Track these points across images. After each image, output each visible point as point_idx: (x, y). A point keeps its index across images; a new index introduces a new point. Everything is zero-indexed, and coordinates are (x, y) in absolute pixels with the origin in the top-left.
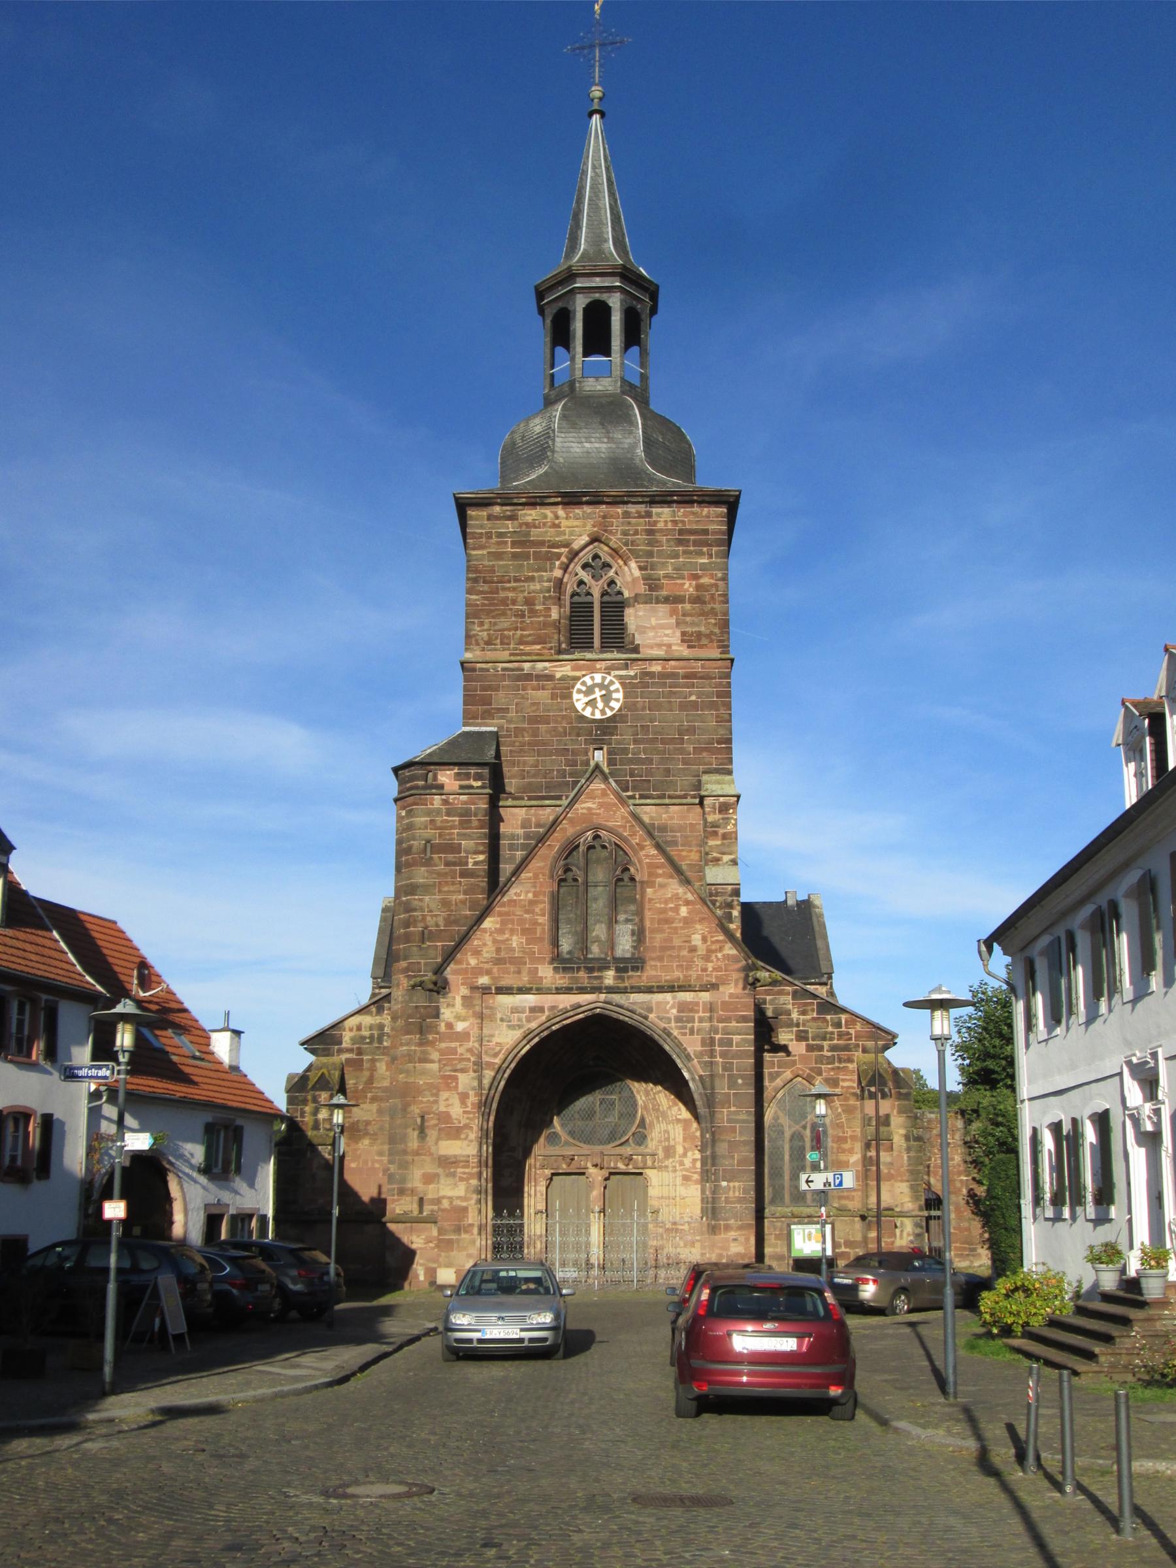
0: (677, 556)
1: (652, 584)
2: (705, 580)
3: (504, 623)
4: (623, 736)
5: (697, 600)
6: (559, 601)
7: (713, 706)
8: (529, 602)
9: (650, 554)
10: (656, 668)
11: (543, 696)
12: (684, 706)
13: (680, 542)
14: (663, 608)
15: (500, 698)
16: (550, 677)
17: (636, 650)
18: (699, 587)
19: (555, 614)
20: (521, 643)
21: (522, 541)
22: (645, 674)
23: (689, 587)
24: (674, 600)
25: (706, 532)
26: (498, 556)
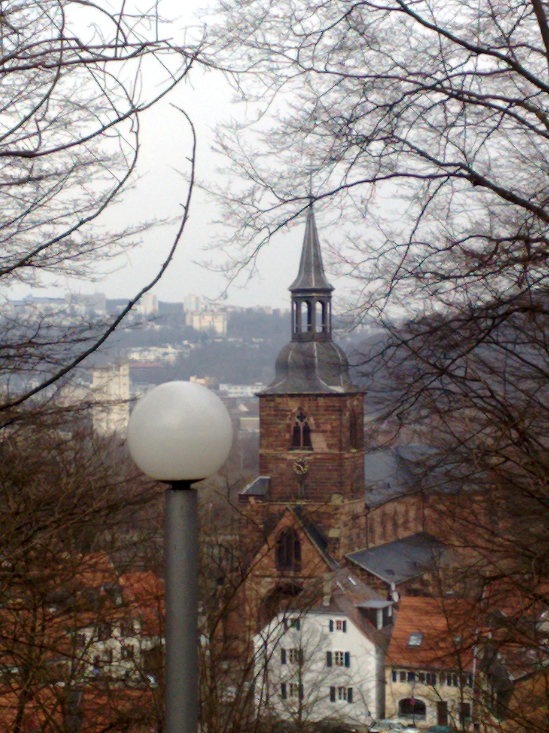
0: (324, 415)
1: (318, 425)
2: (334, 424)
3: (271, 439)
4: (308, 481)
5: (332, 432)
6: (289, 432)
7: (337, 470)
8: (279, 432)
9: (317, 415)
10: (319, 456)
11: (283, 466)
12: (329, 470)
13: (326, 410)
14: (321, 435)
15: (271, 466)
16: (286, 459)
17: (311, 449)
18: (333, 427)
19: (288, 436)
20: (277, 446)
21: (276, 409)
22: (315, 459)
23: (329, 427)
24: (324, 432)
25: (334, 406)
26: (269, 415)
